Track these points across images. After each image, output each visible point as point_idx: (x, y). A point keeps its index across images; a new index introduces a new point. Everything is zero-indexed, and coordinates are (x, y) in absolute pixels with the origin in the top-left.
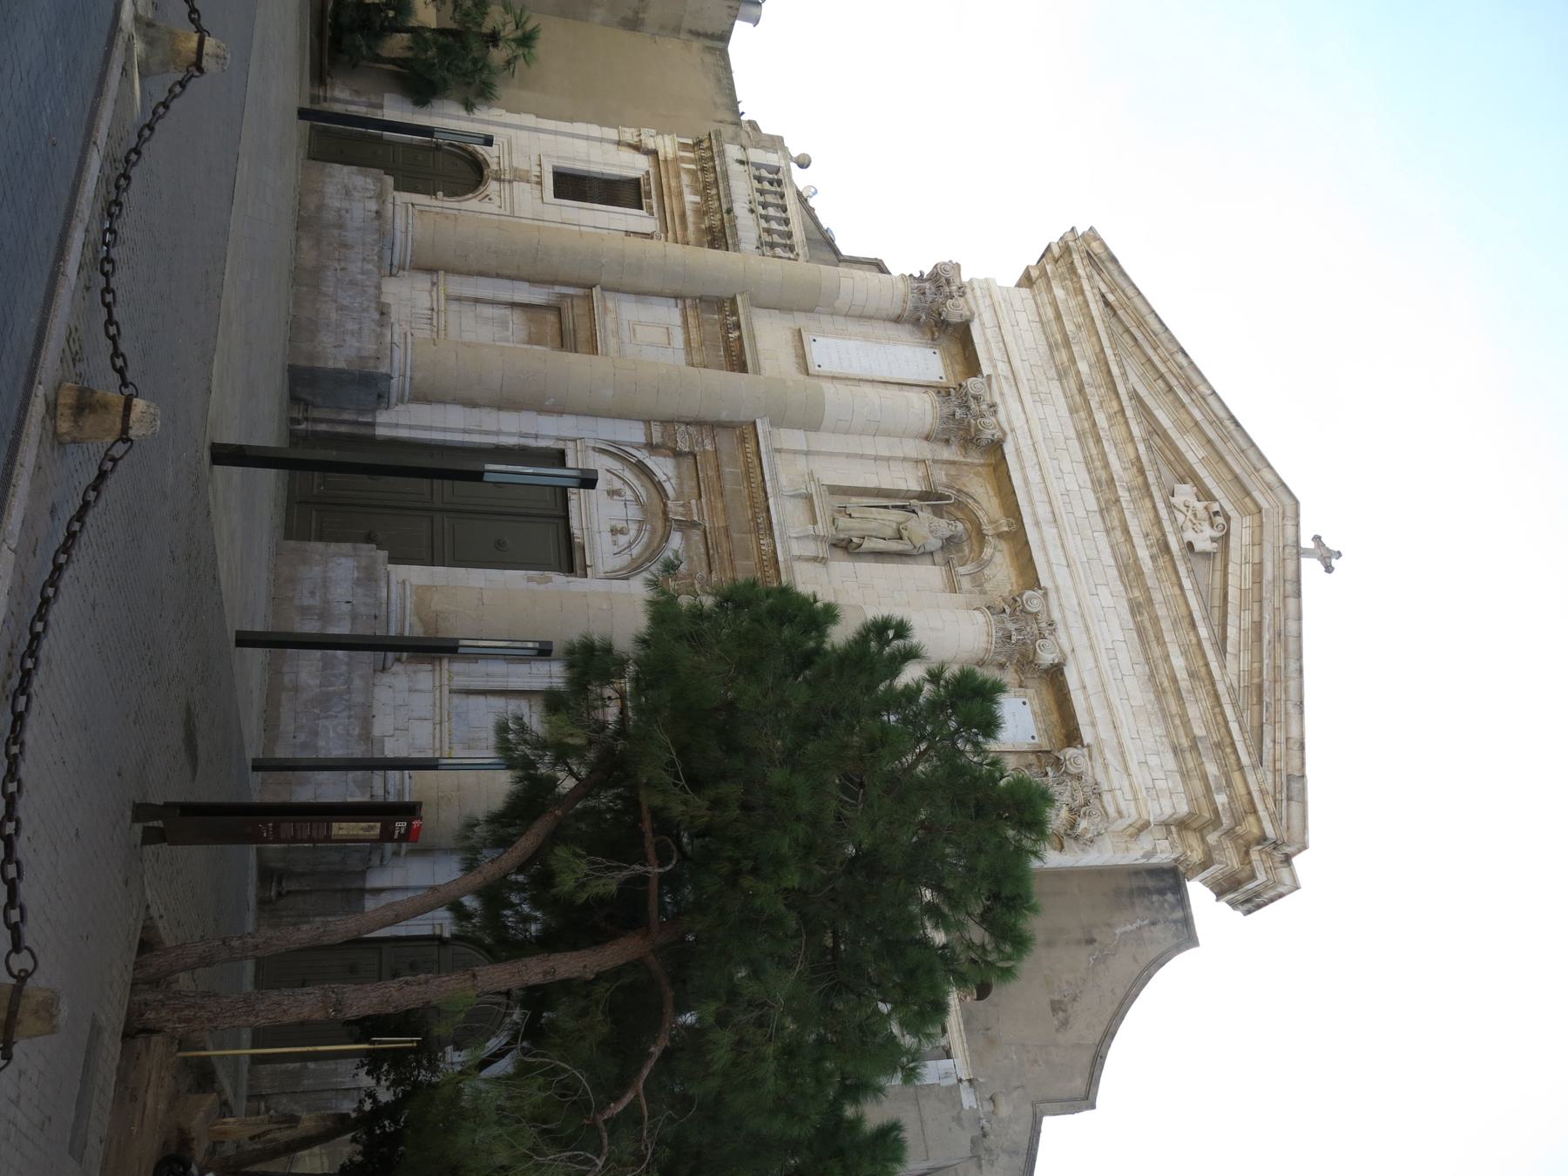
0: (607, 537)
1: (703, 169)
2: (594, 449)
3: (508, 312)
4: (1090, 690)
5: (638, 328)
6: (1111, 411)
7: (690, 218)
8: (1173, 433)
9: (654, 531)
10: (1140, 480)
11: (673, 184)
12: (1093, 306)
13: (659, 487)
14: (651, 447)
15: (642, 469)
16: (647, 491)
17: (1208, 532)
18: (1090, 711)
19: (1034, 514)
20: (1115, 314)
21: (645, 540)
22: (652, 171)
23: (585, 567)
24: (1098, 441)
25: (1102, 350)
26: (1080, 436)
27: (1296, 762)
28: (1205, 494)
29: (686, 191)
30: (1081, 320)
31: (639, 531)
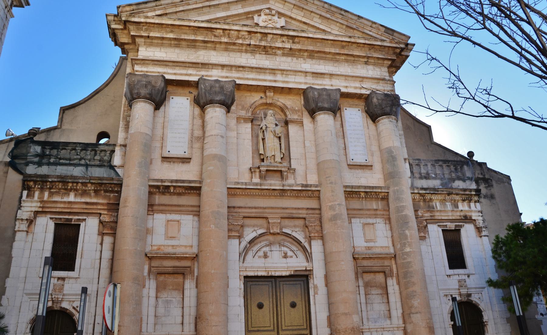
0: (289, 260)
1: (50, 188)
2: (243, 262)
3: (160, 300)
4: (348, 85)
5: (170, 235)
6: (222, 34)
7: (88, 200)
8: (229, 13)
9: (284, 240)
10: (259, 35)
11: (62, 206)
12: (164, 22)
13: (261, 235)
14: (240, 237)
15: (252, 242)
16: (263, 241)
17: (276, 18)
18: (356, 88)
19: (271, 81)
20: (166, 14)
21: (289, 244)
22: (49, 216)
23: (306, 270)
24: (234, 44)
25: (189, 26)
26: (226, 50)
27: (381, 27)
28: (259, 12)
29: (65, 199)
30: (168, 30)
31: (284, 246)
